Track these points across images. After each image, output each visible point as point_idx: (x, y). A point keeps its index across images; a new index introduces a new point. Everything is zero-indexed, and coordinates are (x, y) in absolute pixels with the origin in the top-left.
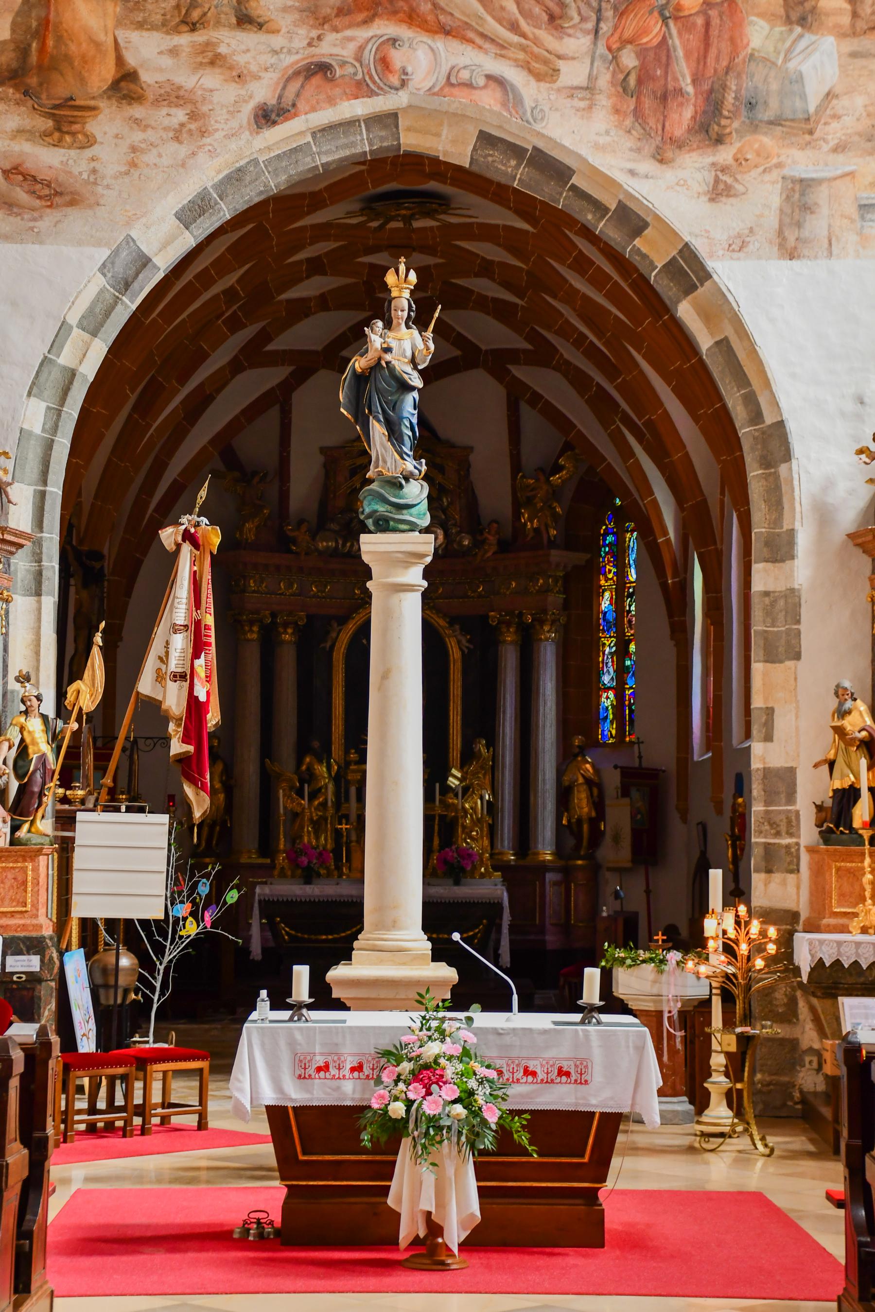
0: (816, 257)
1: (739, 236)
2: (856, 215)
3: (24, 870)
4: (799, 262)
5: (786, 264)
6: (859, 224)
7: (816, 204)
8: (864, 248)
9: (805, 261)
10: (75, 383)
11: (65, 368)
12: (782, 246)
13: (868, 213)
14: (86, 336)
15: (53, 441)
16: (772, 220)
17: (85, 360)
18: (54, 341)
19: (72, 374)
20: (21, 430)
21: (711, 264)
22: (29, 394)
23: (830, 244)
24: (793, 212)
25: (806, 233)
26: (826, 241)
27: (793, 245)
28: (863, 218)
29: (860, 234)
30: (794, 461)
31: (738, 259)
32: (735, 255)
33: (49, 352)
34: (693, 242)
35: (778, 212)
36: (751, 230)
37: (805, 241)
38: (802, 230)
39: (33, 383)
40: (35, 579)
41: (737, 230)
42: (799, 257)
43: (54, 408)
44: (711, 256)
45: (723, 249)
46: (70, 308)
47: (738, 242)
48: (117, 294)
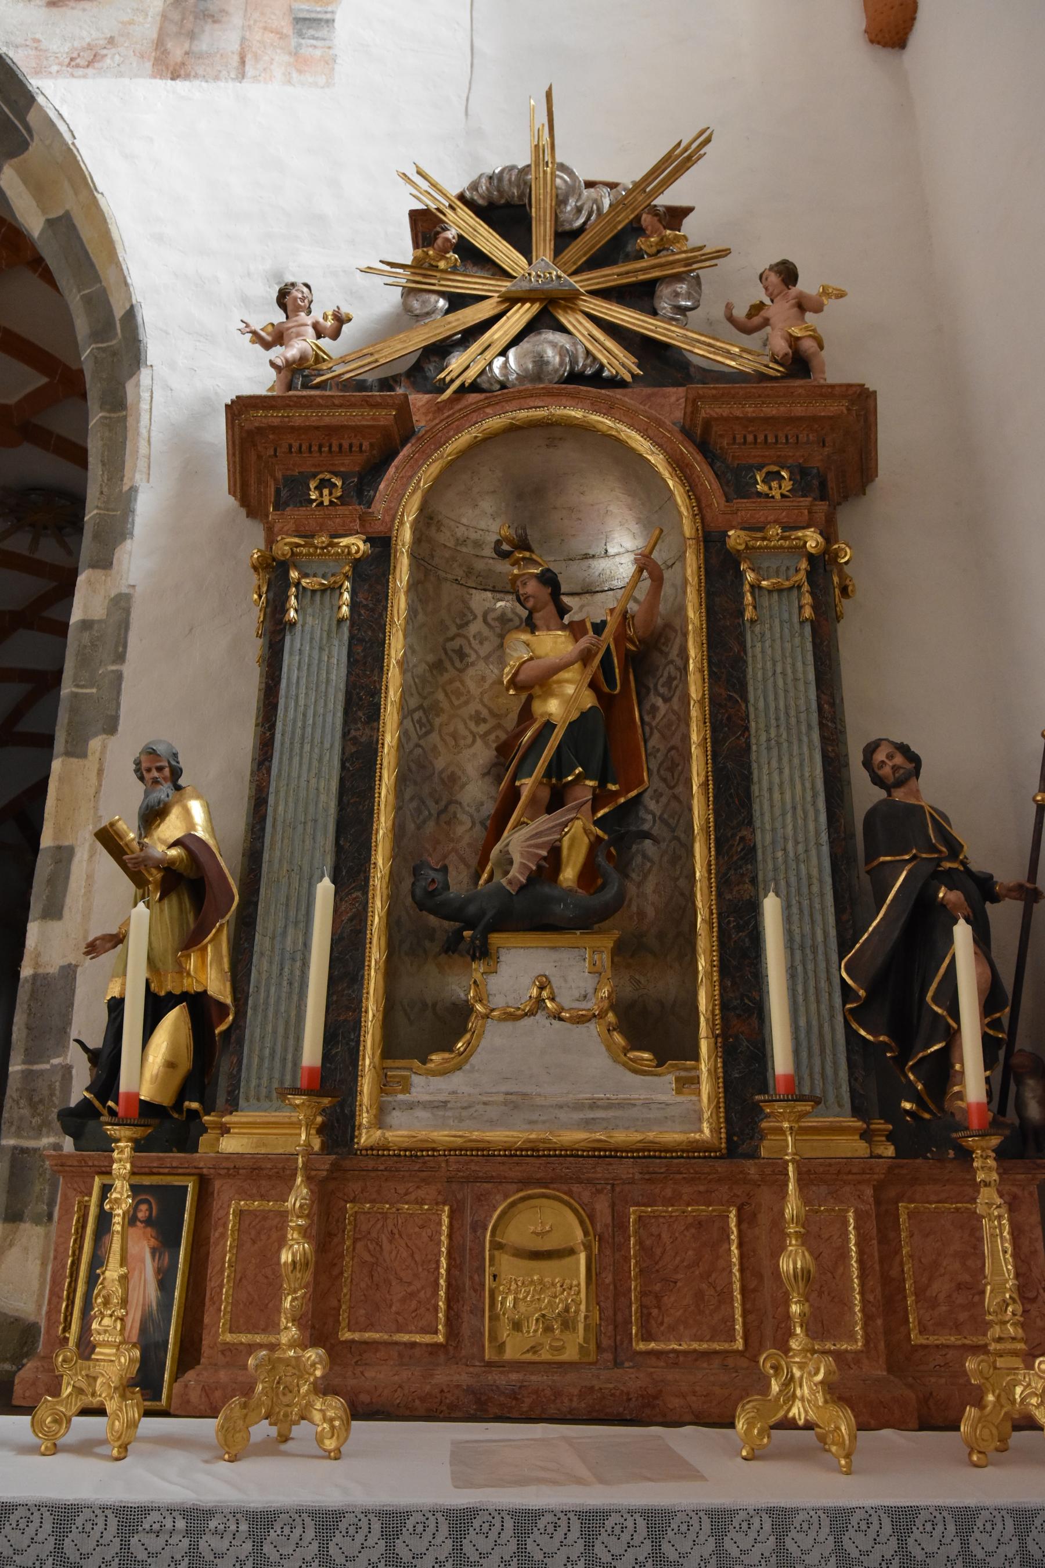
0: (217, 78)
1: (89, 47)
2: (288, 29)
4: (187, 83)
5: (164, 86)
6: (294, 41)
7: (222, 11)
8: (300, 72)
9: (197, 83)
12: (158, 62)
13: (309, 28)
16: (147, 29)
21: (34, 83)
23: (243, 62)
24: (183, 20)
25: (203, 45)
26: (236, 58)
27: (179, 60)
28: (300, 34)
29: (295, 54)
30: (144, 375)
31: (85, 76)
32: (80, 72)
34: (11, 54)
35: (158, 18)
36: (111, 41)
37: (200, 56)
38: (196, 42)
41: (88, 40)
42: (187, 77)
44: (37, 73)
45: (61, 64)
47: (88, 55)
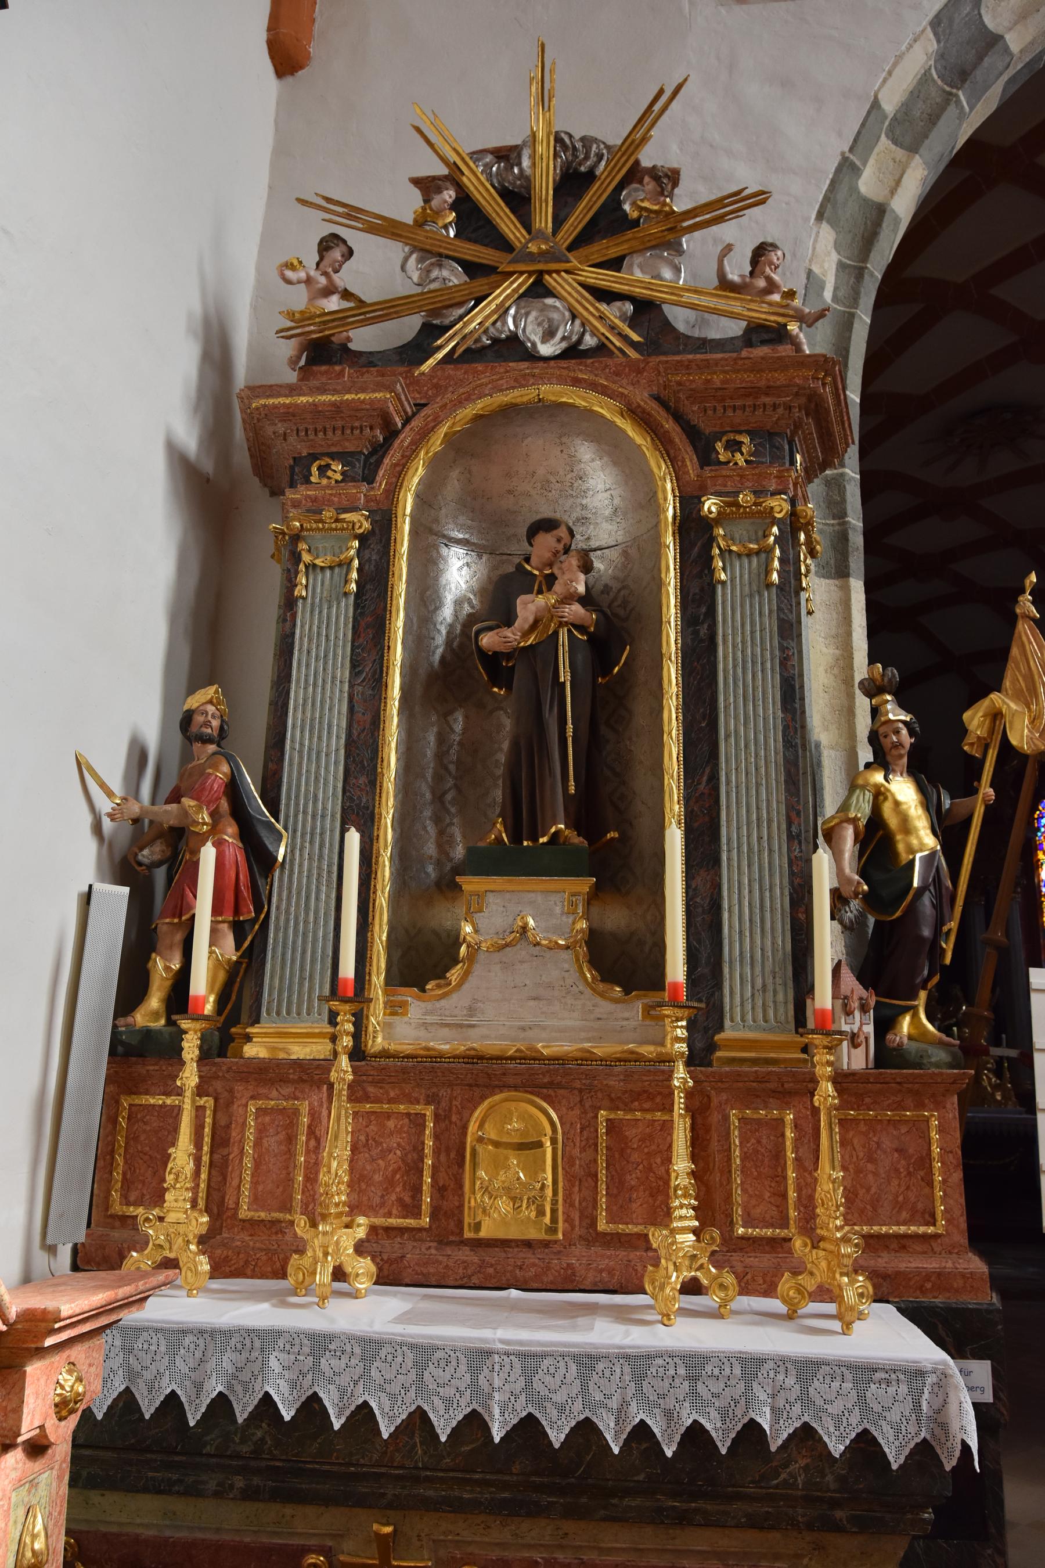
3: (921, 1128)
10: (884, 225)
11: (866, 201)
14: (900, 153)
15: (852, 315)
17: (899, 190)
18: (859, 133)
19: (879, 211)
20: (810, 273)
22: (820, 216)
33: (851, 150)
39: (826, 199)
40: (834, 548)
43: (849, 266)
46: (885, 81)
48: (948, 89)
